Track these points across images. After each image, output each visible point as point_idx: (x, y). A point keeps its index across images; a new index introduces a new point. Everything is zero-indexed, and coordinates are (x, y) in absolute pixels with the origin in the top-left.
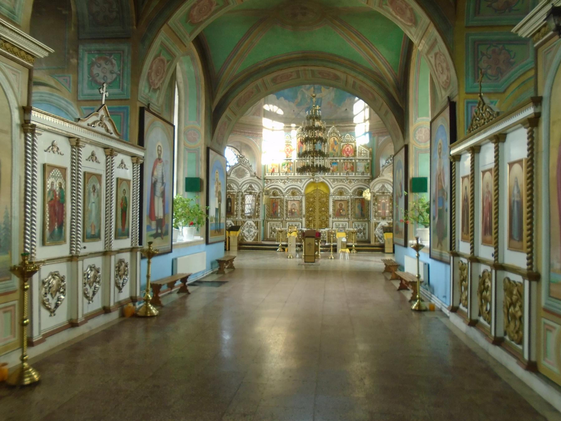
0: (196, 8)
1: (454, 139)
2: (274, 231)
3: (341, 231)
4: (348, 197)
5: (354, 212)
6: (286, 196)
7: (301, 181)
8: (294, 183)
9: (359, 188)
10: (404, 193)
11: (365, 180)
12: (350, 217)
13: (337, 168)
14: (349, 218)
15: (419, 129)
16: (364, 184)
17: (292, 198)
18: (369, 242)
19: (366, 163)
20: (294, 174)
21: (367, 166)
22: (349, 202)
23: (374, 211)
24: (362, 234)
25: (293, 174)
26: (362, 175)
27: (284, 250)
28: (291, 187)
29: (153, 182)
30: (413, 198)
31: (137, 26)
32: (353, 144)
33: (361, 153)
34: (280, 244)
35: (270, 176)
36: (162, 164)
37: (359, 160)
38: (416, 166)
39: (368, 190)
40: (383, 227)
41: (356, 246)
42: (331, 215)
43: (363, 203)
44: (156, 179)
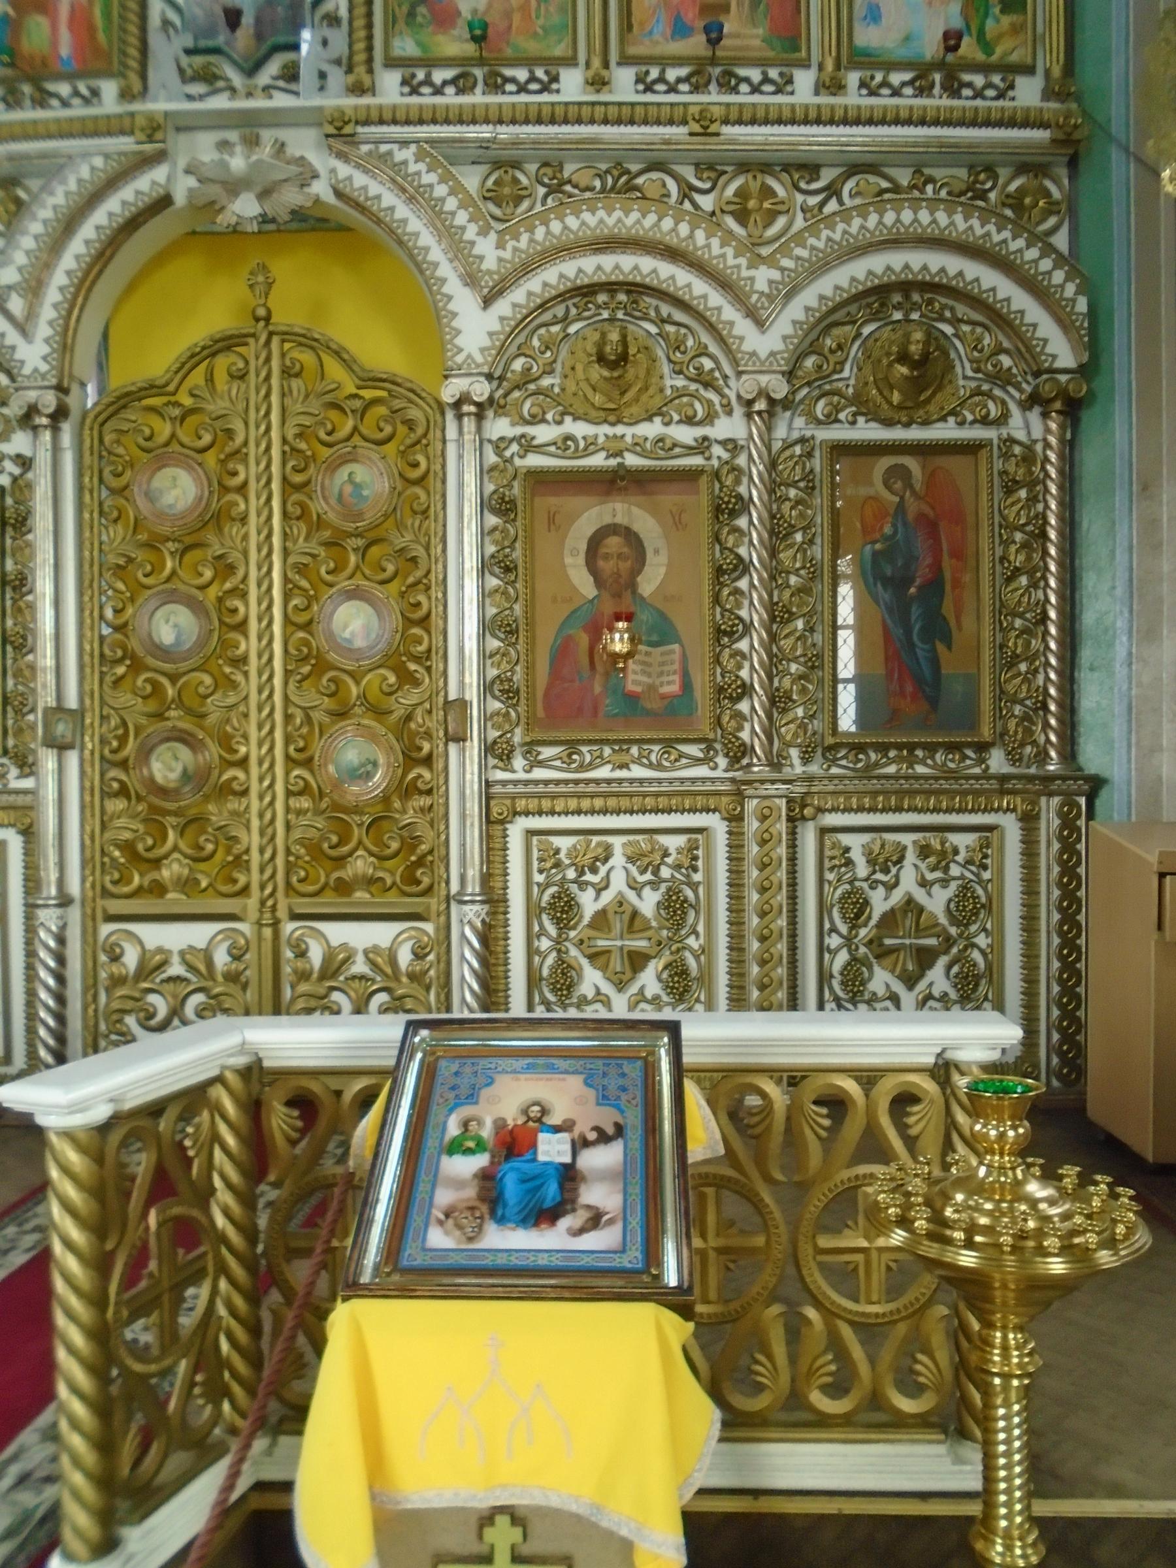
14: (739, 754)
16: (960, 224)
22: (742, 505)
42: (463, 704)
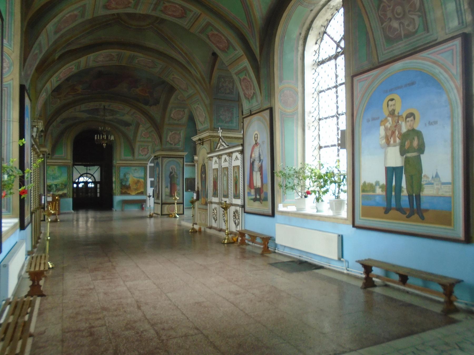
0: (218, 45)
29: (251, 162)
36: (259, 146)
44: (253, 159)
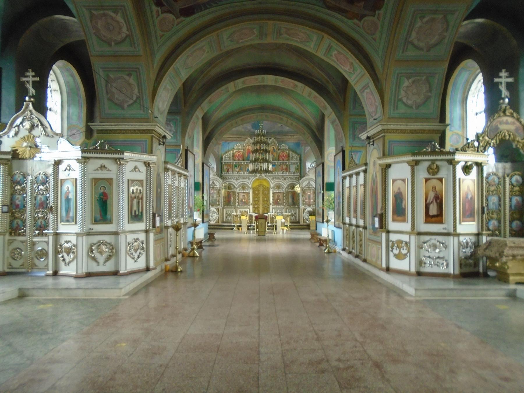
1: (344, 169)
2: (229, 215)
3: (279, 215)
4: (284, 190)
5: (288, 201)
6: (238, 190)
7: (249, 179)
8: (243, 180)
9: (291, 184)
10: (322, 191)
11: (296, 178)
12: (285, 205)
13: (276, 169)
14: (284, 206)
15: (331, 154)
16: (295, 181)
17: (242, 191)
18: (299, 223)
19: (296, 166)
20: (244, 173)
21: (297, 168)
23: (302, 201)
24: (294, 217)
25: (243, 173)
26: (293, 174)
27: (239, 229)
28: (242, 182)
30: (326, 194)
31: (185, 106)
32: (287, 151)
33: (293, 158)
34: (236, 225)
35: (226, 174)
37: (291, 163)
38: (329, 175)
39: (298, 186)
40: (309, 211)
41: (290, 226)
43: (294, 195)
